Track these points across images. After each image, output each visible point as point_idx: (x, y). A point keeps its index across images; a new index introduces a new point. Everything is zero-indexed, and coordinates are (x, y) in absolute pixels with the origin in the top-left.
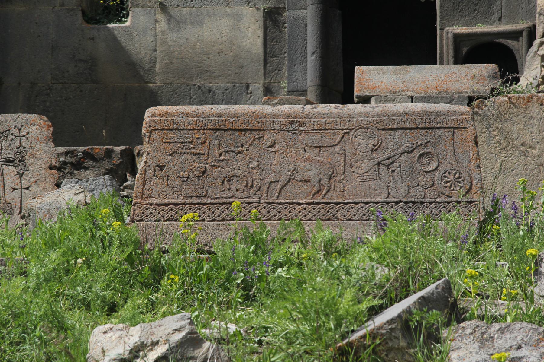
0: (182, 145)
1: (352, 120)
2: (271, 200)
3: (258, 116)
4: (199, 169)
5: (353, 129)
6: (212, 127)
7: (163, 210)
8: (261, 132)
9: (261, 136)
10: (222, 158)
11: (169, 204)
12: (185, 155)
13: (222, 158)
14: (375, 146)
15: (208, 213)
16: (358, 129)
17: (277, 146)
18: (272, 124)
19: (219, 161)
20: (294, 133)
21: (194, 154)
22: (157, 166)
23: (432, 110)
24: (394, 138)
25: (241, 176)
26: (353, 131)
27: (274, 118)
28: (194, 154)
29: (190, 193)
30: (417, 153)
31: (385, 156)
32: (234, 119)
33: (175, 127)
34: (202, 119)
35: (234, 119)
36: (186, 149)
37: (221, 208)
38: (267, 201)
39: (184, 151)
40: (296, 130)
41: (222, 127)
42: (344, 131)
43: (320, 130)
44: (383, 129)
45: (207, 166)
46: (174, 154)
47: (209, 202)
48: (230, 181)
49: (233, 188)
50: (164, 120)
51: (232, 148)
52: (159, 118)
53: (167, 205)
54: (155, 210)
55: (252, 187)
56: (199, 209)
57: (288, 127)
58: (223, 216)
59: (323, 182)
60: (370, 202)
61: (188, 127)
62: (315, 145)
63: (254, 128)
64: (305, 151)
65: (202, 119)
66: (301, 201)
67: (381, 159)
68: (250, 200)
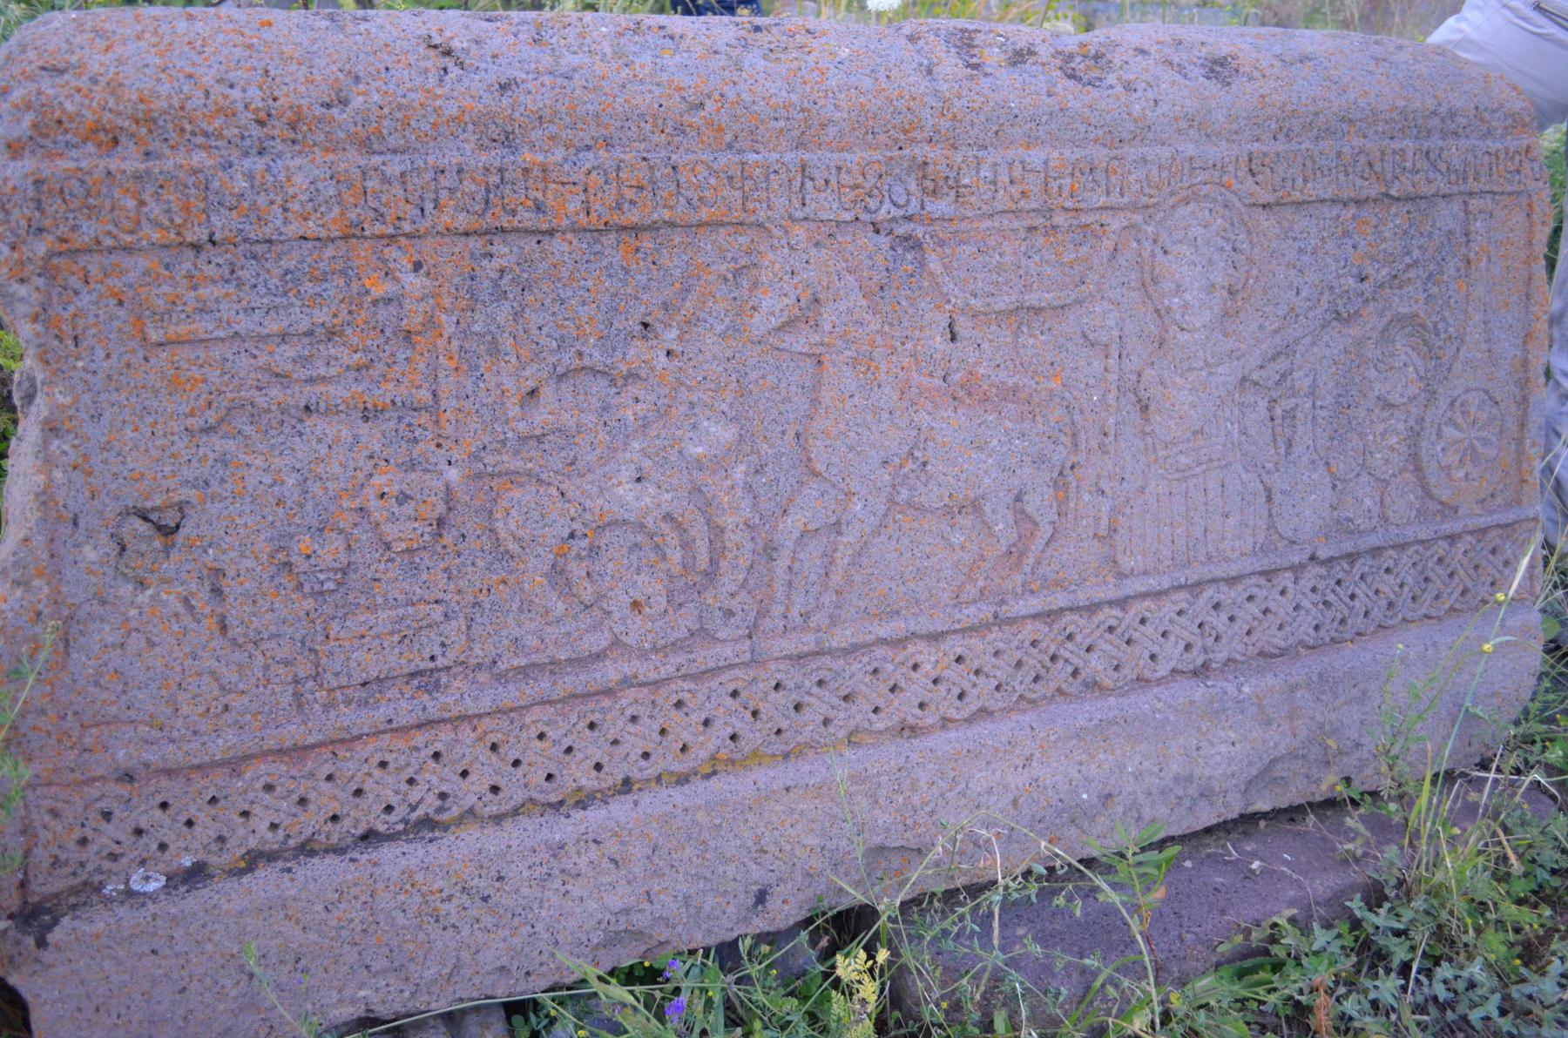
1: (1151, 152)
4: (408, 509)
6: (462, 221)
12: (316, 425)
18: (797, 183)
19: (523, 439)
22: (127, 513)
25: (650, 521)
35: (589, 160)
36: (311, 381)
40: (909, 218)
41: (526, 218)
49: (619, 602)
51: (596, 357)
52: (89, 159)
55: (711, 575)
57: (872, 204)
59: (1032, 505)
61: (312, 228)
68: (706, 657)
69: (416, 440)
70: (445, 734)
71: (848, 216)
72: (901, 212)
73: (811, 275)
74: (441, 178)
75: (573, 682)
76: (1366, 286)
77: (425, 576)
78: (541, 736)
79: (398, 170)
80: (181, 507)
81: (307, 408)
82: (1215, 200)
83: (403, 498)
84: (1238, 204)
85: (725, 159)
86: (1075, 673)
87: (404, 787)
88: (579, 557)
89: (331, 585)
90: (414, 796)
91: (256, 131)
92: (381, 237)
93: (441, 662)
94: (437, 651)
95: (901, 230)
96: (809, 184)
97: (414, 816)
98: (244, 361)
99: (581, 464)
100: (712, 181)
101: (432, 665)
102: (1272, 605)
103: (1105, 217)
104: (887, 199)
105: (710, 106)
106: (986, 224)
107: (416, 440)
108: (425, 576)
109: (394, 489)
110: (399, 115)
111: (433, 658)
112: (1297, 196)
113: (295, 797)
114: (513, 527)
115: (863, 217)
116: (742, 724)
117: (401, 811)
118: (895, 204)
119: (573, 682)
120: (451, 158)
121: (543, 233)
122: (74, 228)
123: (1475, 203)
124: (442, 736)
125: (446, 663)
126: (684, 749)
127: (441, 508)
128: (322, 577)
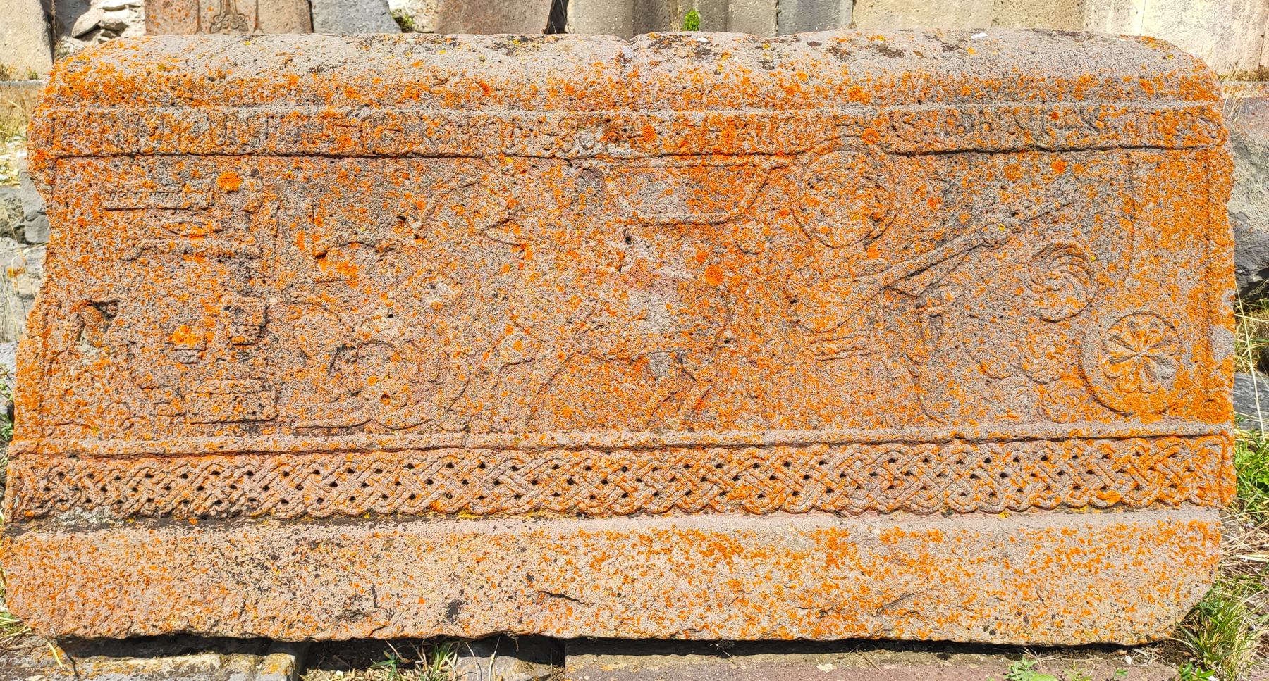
0: (171, 220)
2: (507, 438)
3: (454, 100)
5: (801, 152)
7: (118, 478)
8: (470, 166)
9: (469, 180)
10: (324, 270)
11: (139, 456)
13: (324, 270)
14: (877, 220)
15: (281, 488)
16: (820, 154)
17: (529, 221)
19: (317, 282)
20: (590, 170)
21: (223, 257)
22: (89, 303)
23: (1088, 73)
24: (945, 192)
25: (396, 343)
26: (804, 159)
27: (512, 106)
28: (223, 257)
29: (209, 409)
30: (1026, 247)
31: (912, 264)
32: (366, 112)
33: (145, 143)
34: (244, 113)
37: (331, 468)
38: (491, 439)
39: (183, 243)
42: (774, 161)
43: (683, 155)
44: (909, 155)
45: (273, 301)
46: (147, 257)
47: (282, 446)
48: (356, 360)
49: (373, 391)
50: (103, 116)
53: (132, 457)
54: (91, 476)
56: (250, 474)
57: (566, 146)
58: (336, 500)
60: (850, 443)
61: (193, 148)
62: (665, 218)
63: (441, 148)
64: (628, 240)
65: (244, 113)
66: (607, 441)
67: (897, 271)
69: (250, 278)
70: (256, 460)
71: (546, 154)
72: (588, 153)
73: (516, 192)
74: (271, 121)
75: (342, 440)
76: (1015, 220)
77: (252, 361)
78: (317, 472)
79: (246, 116)
80: (115, 303)
81: (186, 252)
82: (858, 149)
83: (238, 311)
84: (881, 153)
85: (456, 114)
86: (723, 493)
87: (228, 490)
88: (348, 361)
89: (194, 359)
90: (235, 496)
91: (171, 94)
92: (233, 154)
93: (259, 416)
94: (258, 410)
95: (586, 164)
96: (518, 132)
97: (233, 510)
98: (152, 222)
99: (353, 303)
100: (447, 127)
101: (253, 418)
102: (914, 470)
103: (757, 159)
104: (577, 143)
105: (453, 80)
106: (656, 162)
107: (250, 278)
108: (252, 361)
109: (234, 305)
110: (251, 84)
111: (254, 413)
112: (940, 147)
113: (162, 484)
114: (306, 335)
115: (558, 154)
116: (454, 486)
117: (225, 505)
118: (584, 147)
119: (342, 440)
120: (281, 109)
121: (334, 157)
122: (69, 144)
123: (1136, 155)
124: (253, 462)
125: (263, 417)
126: (412, 497)
127: (262, 319)
128: (190, 353)
